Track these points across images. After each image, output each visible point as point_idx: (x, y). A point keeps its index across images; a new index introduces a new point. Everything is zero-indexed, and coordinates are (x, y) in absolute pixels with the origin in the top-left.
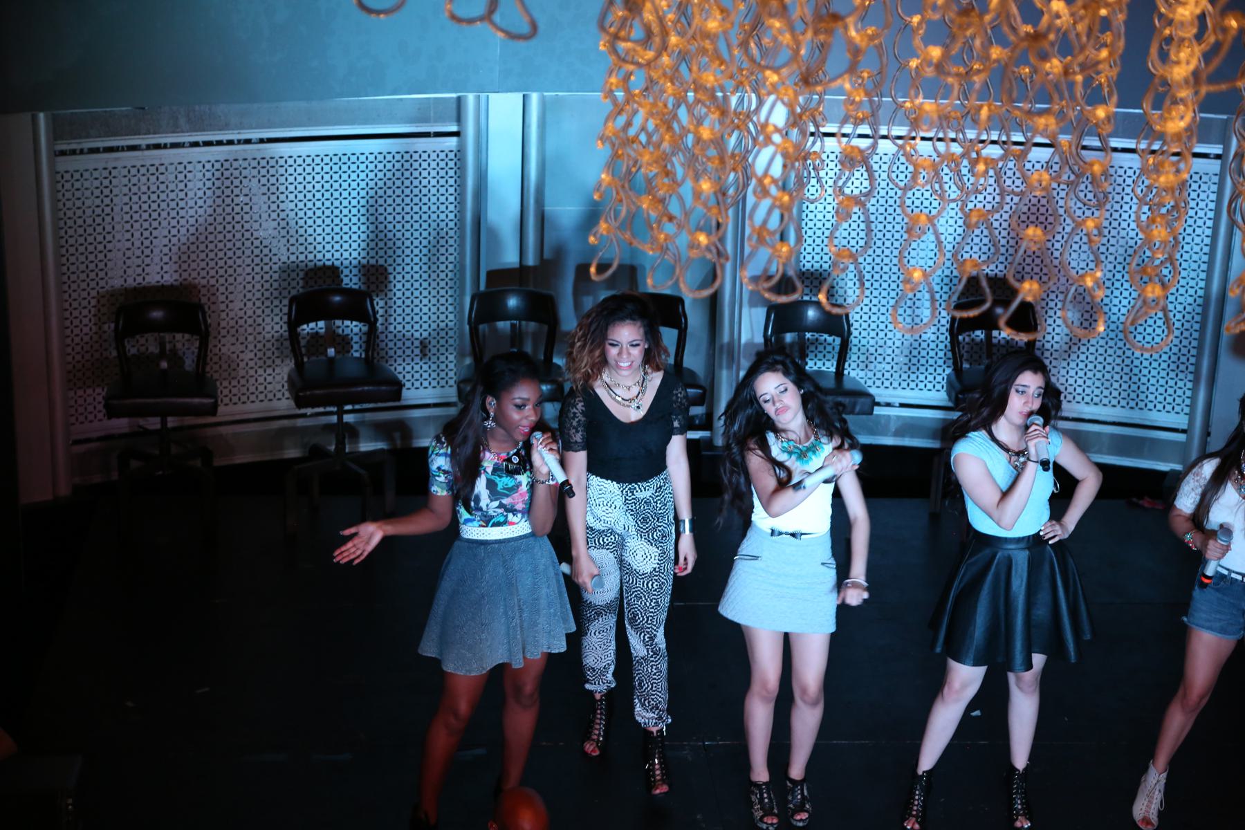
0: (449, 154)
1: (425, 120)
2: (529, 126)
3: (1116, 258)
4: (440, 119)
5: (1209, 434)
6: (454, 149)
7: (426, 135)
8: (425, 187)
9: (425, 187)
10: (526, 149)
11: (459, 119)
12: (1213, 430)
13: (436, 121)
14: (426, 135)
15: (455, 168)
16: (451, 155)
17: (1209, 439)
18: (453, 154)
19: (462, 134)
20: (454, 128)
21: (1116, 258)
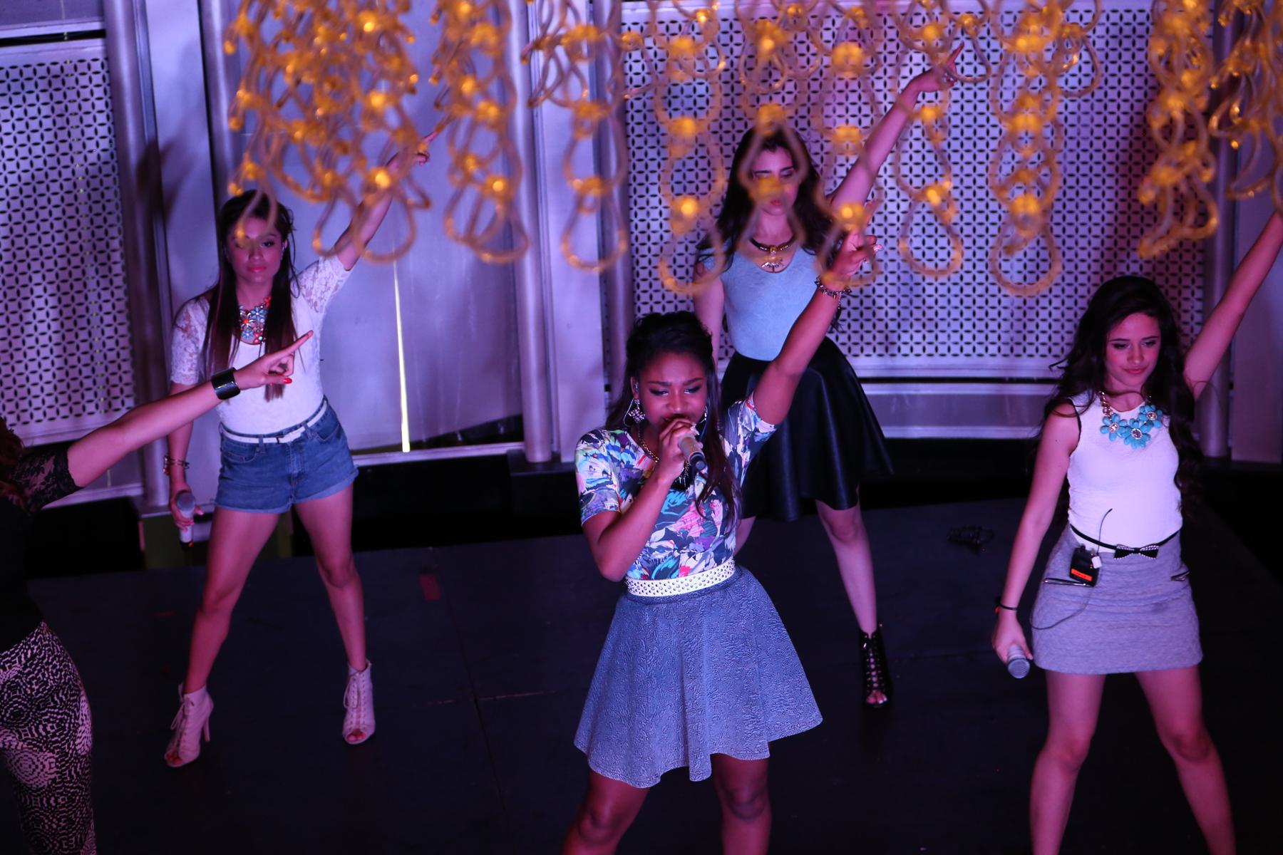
0: (93, 64)
1: (54, 16)
2: (210, 15)
3: (1078, 144)
4: (74, 14)
5: (1231, 386)
6: (101, 57)
7: (57, 38)
8: (61, 116)
9: (61, 116)
10: (209, 50)
11: (102, 11)
12: (1238, 379)
13: (68, 17)
14: (57, 38)
15: (104, 85)
16: (96, 66)
17: (1232, 393)
18: (99, 63)
19: (108, 33)
20: (96, 26)
21: (1078, 144)
